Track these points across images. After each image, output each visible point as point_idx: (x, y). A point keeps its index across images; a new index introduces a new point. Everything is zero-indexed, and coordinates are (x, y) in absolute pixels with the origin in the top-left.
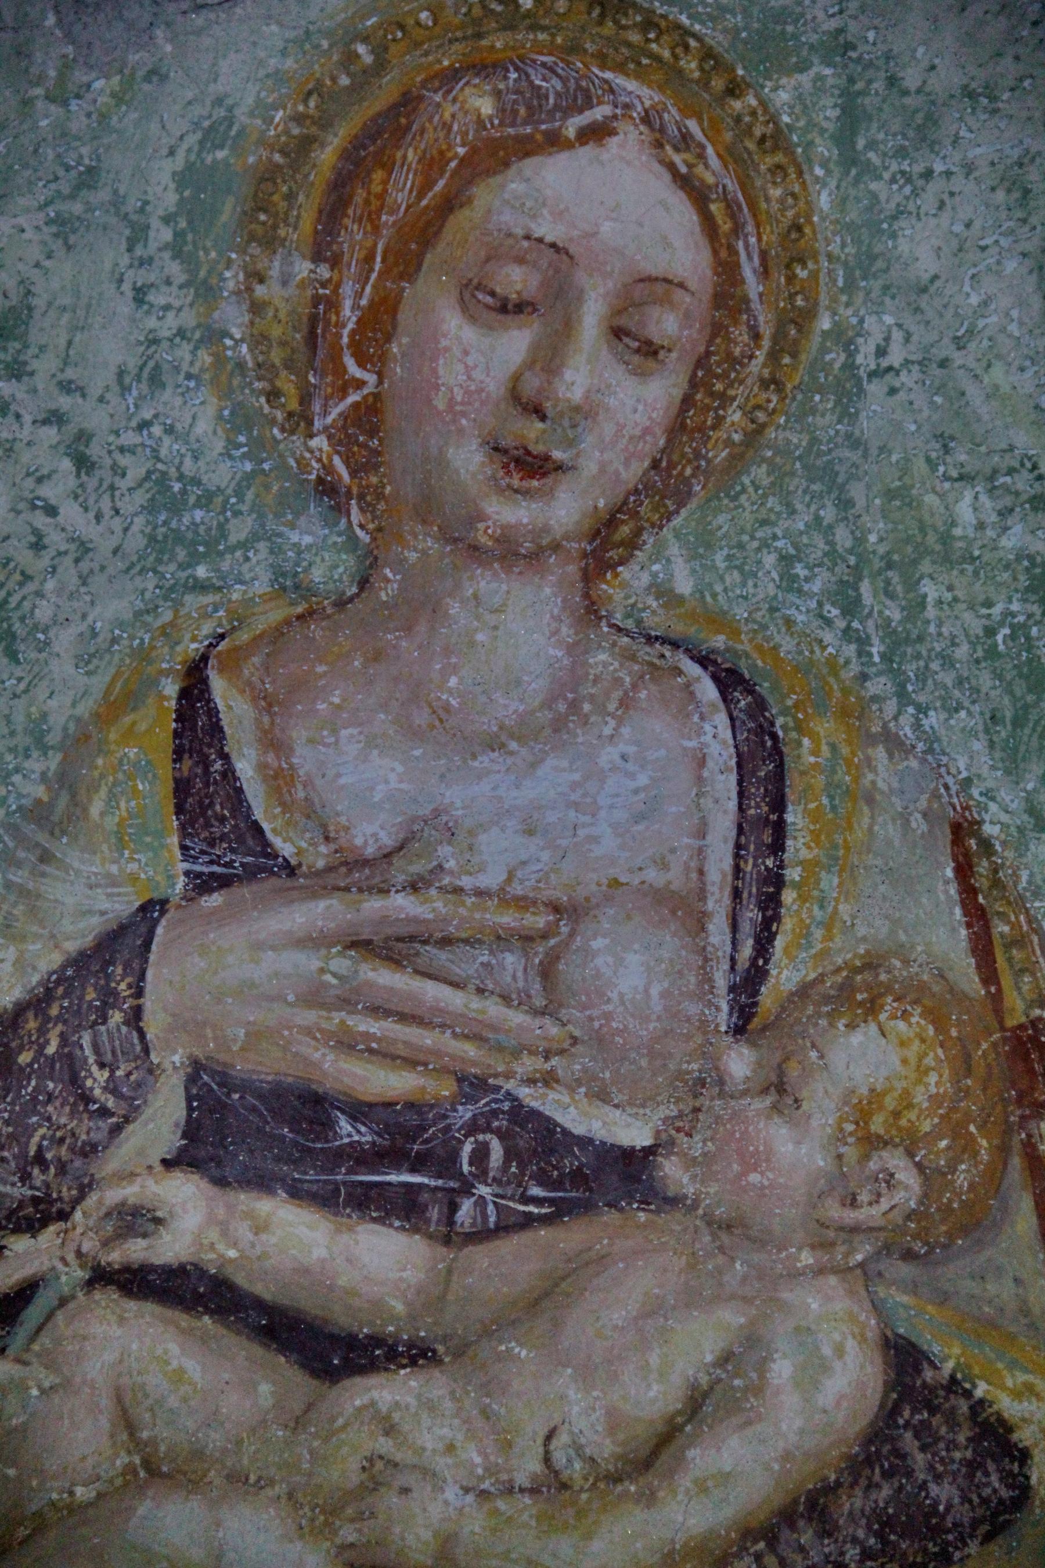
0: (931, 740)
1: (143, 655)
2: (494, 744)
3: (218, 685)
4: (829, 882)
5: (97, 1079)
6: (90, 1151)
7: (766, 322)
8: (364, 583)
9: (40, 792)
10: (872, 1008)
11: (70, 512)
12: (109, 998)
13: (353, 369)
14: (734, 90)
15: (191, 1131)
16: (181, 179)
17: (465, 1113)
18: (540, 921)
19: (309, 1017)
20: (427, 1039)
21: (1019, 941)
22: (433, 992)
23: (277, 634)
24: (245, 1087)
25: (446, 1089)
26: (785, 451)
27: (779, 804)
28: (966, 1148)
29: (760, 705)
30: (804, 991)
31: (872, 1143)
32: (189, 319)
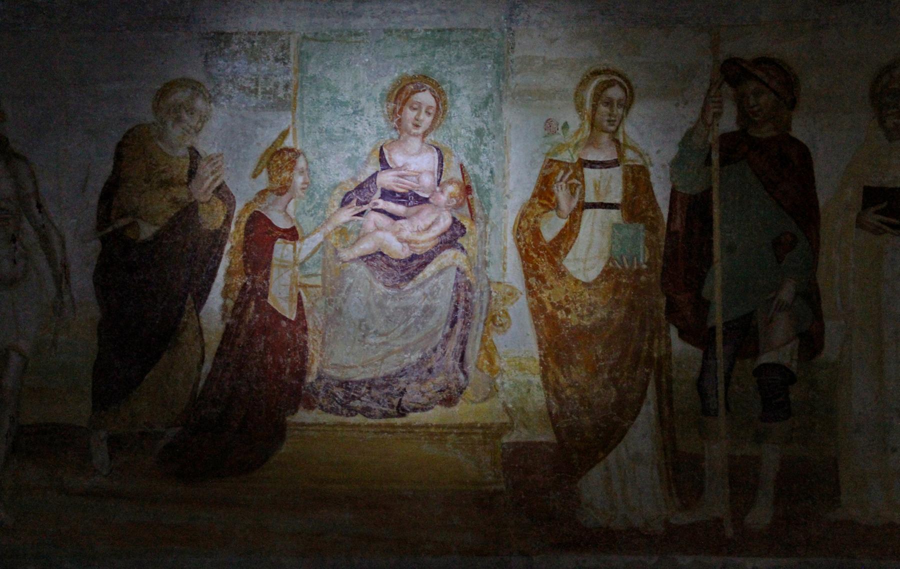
0: (458, 156)
1: (376, 145)
2: (413, 155)
3: (384, 149)
4: (447, 170)
5: (372, 189)
6: (371, 197)
7: (442, 111)
8: (399, 138)
9: (365, 160)
10: (452, 184)
11: (368, 130)
12: (373, 181)
13: (398, 115)
14: (439, 86)
15: (382, 195)
16: (381, 94)
17: (409, 194)
18: (417, 174)
19: (393, 183)
20: (405, 186)
21: (467, 177)
22: (406, 181)
23: (390, 143)
24: (387, 190)
25: (408, 191)
26: (444, 125)
27: (442, 162)
28: (461, 198)
29: (441, 152)
30: (445, 182)
31: (451, 197)
32: (381, 110)
